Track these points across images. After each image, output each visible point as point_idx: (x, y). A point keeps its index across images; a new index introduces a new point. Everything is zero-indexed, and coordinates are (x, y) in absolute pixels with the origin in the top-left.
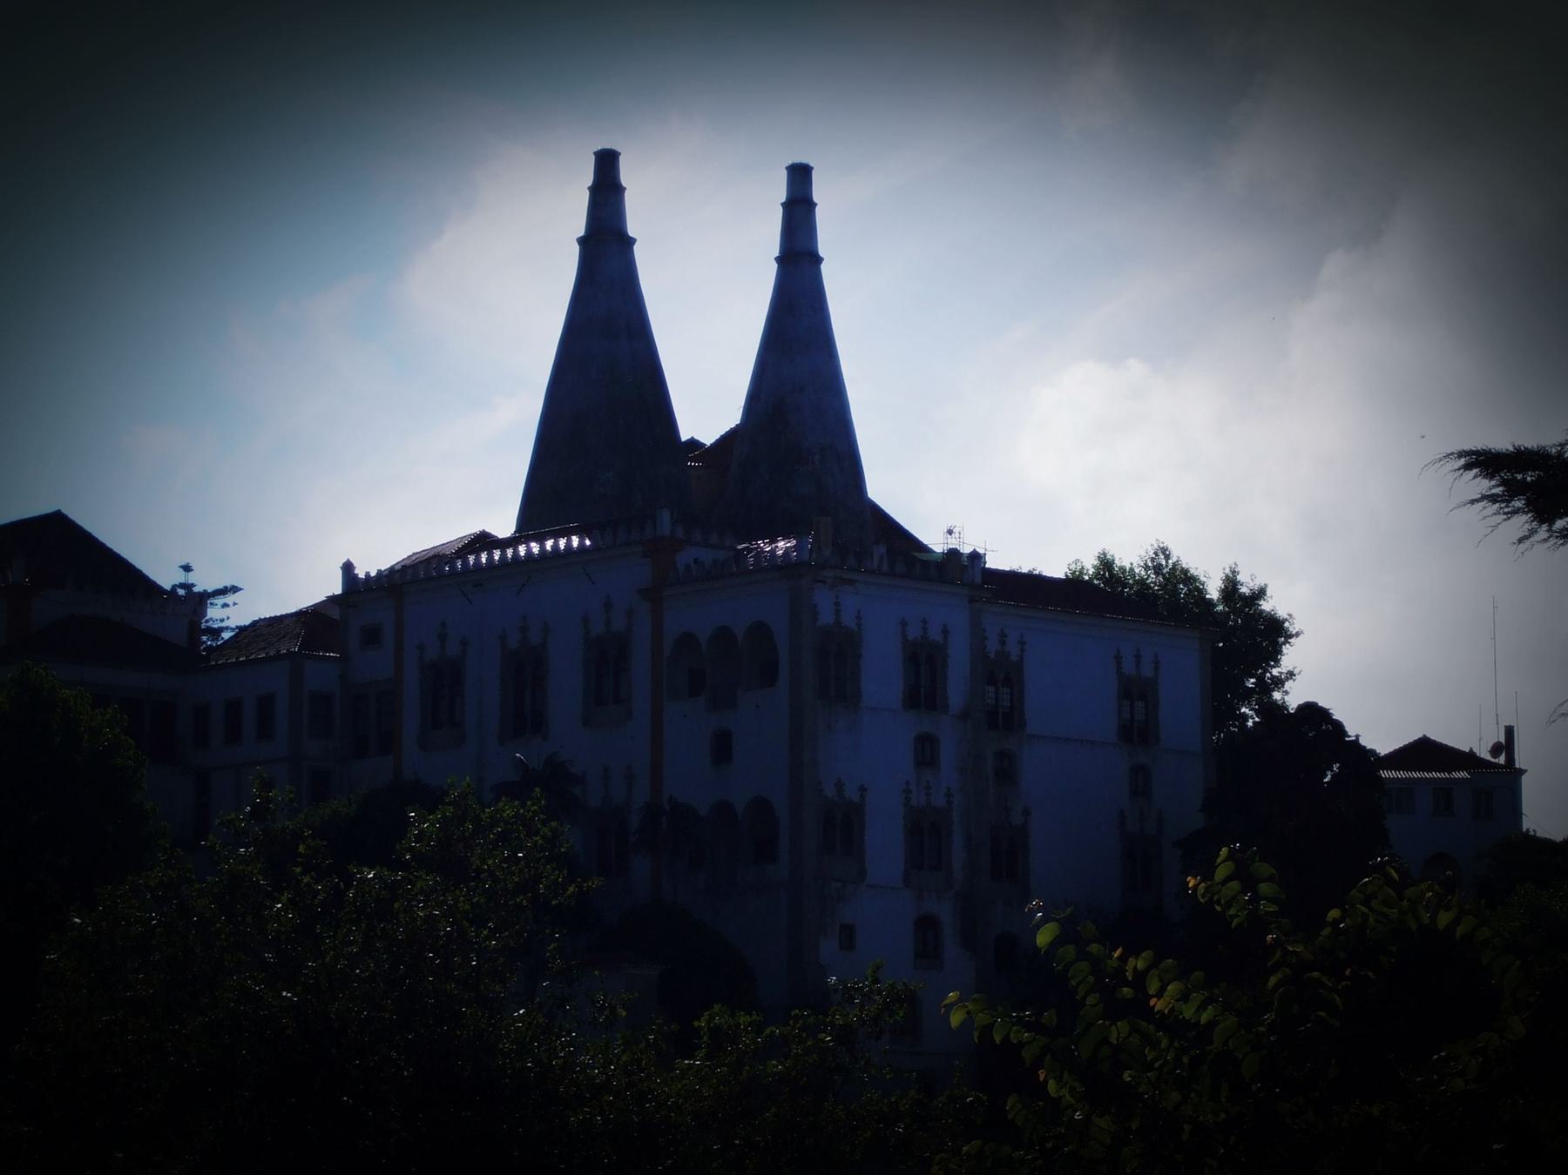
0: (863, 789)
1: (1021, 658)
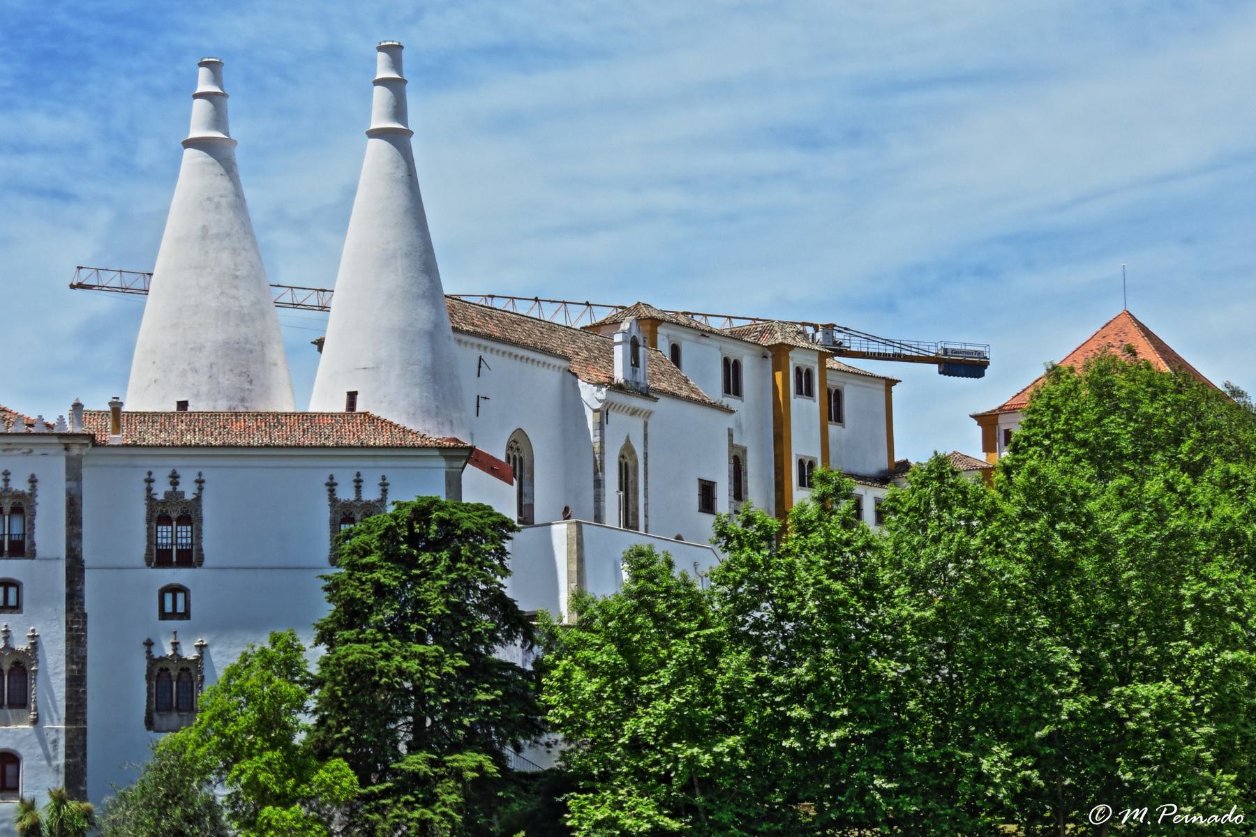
1: (198, 499)
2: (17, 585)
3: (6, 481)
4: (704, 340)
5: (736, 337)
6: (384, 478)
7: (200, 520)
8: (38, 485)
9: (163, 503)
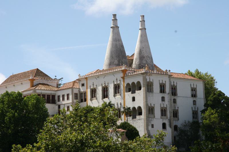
0: (154, 105)
1: (176, 86)
3: (162, 81)
8: (166, 82)
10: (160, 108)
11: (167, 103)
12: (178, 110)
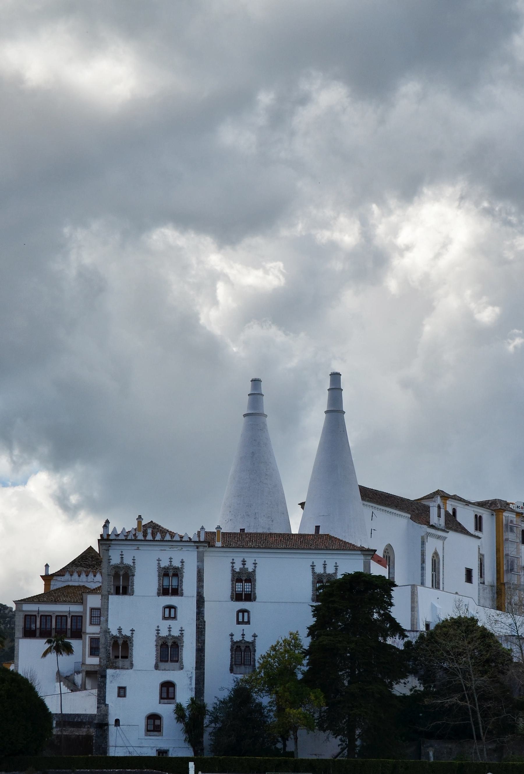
1: (254, 571)
2: (174, 607)
4: (467, 507)
5: (481, 504)
6: (336, 563)
7: (255, 580)
9: (238, 573)
10: (155, 638)
11: (185, 623)
12: (253, 643)
